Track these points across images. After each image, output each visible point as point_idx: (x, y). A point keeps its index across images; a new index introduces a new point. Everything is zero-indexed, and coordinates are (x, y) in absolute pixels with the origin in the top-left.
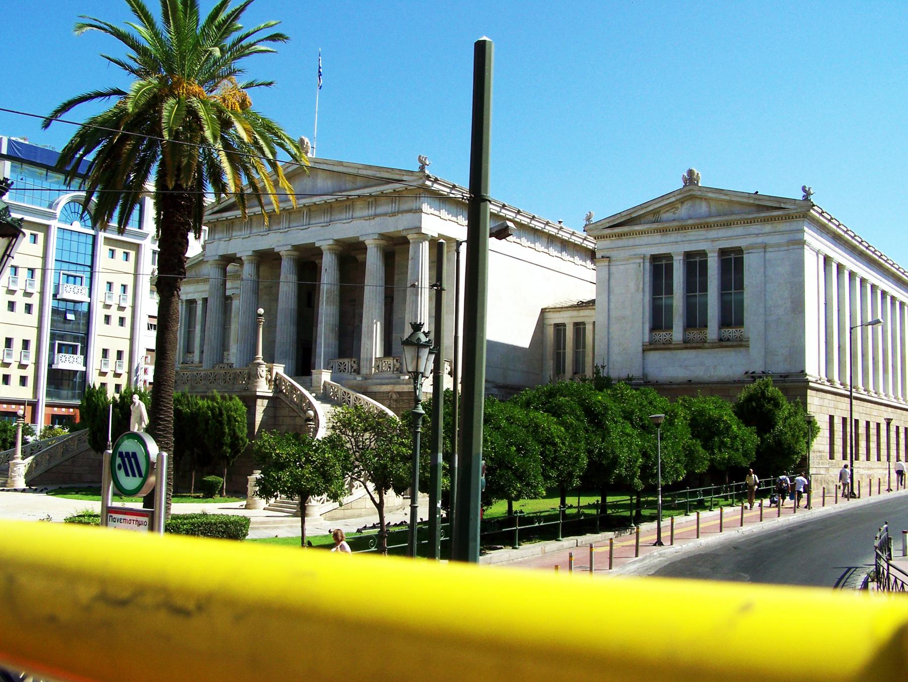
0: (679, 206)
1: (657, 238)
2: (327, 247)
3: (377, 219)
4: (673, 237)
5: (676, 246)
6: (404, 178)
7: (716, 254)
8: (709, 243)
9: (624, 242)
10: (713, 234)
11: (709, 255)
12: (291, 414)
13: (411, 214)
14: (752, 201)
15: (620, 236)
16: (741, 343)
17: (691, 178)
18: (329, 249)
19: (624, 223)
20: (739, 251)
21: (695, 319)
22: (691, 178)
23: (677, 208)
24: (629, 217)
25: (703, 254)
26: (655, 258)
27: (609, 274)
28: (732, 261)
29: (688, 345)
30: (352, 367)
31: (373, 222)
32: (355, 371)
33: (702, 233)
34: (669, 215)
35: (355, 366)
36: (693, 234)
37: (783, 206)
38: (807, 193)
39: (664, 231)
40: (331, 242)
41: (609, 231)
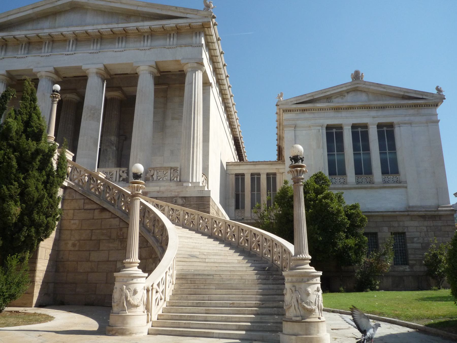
0: (346, 94)
1: (332, 114)
2: (95, 71)
3: (152, 50)
4: (344, 114)
5: (346, 121)
6: (188, 16)
7: (376, 126)
8: (371, 120)
9: (306, 115)
10: (373, 113)
11: (370, 127)
12: (87, 207)
13: (191, 47)
14: (402, 93)
15: (304, 110)
16: (401, 184)
17: (357, 76)
18: (97, 73)
19: (309, 103)
20: (391, 126)
21: (364, 169)
22: (357, 76)
23: (345, 96)
24: (311, 98)
25: (365, 126)
26: (329, 128)
27: (295, 136)
28: (387, 133)
29: (359, 186)
30: (120, 176)
31: (148, 52)
32: (123, 180)
33: (365, 112)
34: (339, 99)
35: (124, 176)
36: (358, 113)
37: (424, 97)
38: (439, 90)
39: (337, 109)
40: (101, 66)
41: (295, 106)
